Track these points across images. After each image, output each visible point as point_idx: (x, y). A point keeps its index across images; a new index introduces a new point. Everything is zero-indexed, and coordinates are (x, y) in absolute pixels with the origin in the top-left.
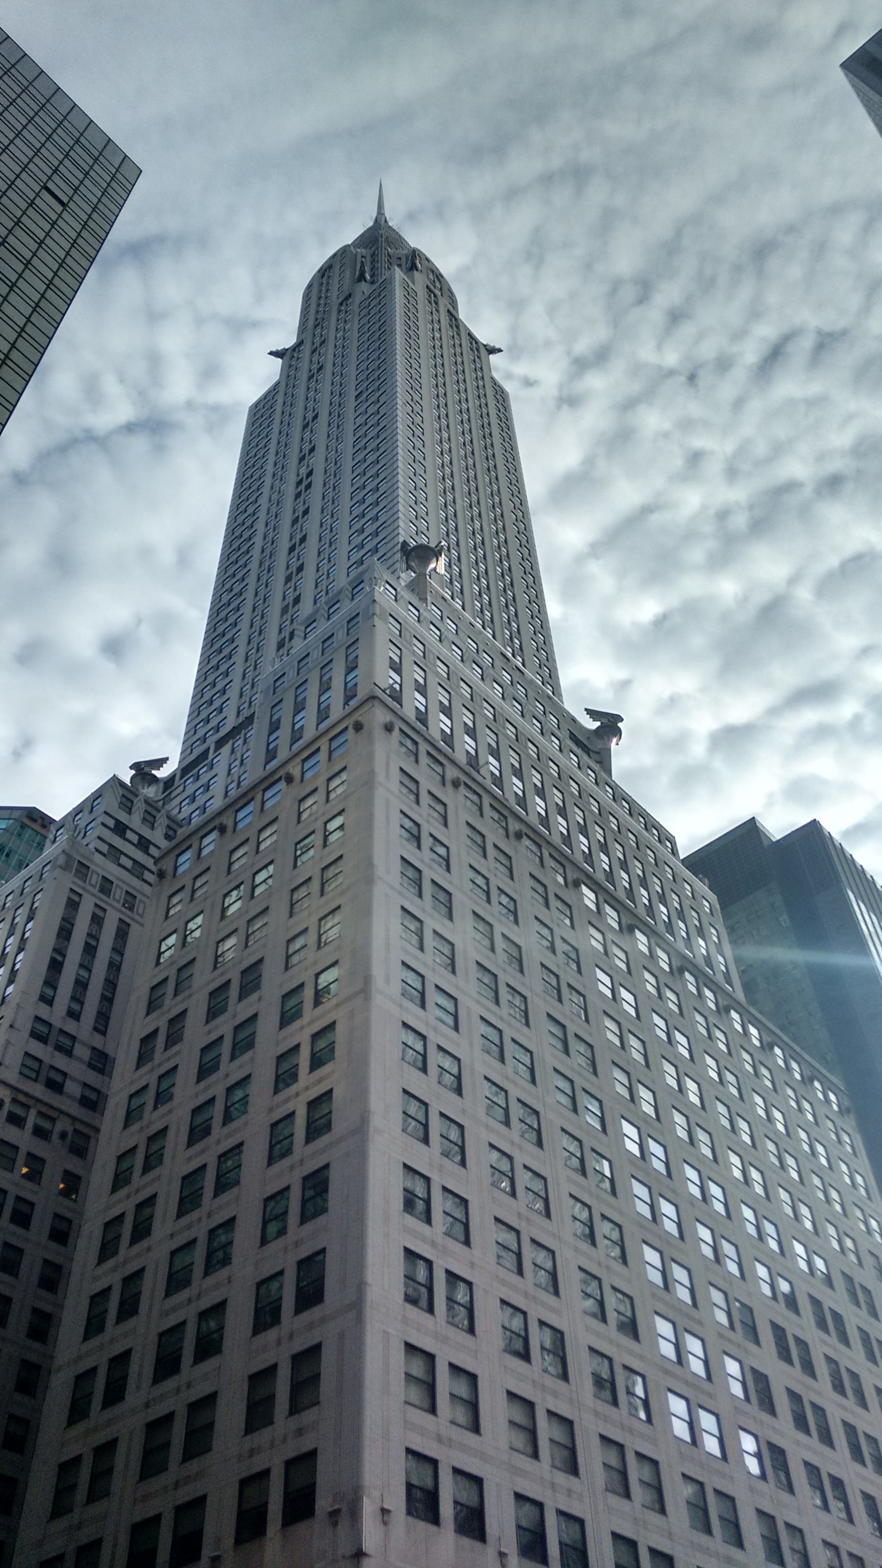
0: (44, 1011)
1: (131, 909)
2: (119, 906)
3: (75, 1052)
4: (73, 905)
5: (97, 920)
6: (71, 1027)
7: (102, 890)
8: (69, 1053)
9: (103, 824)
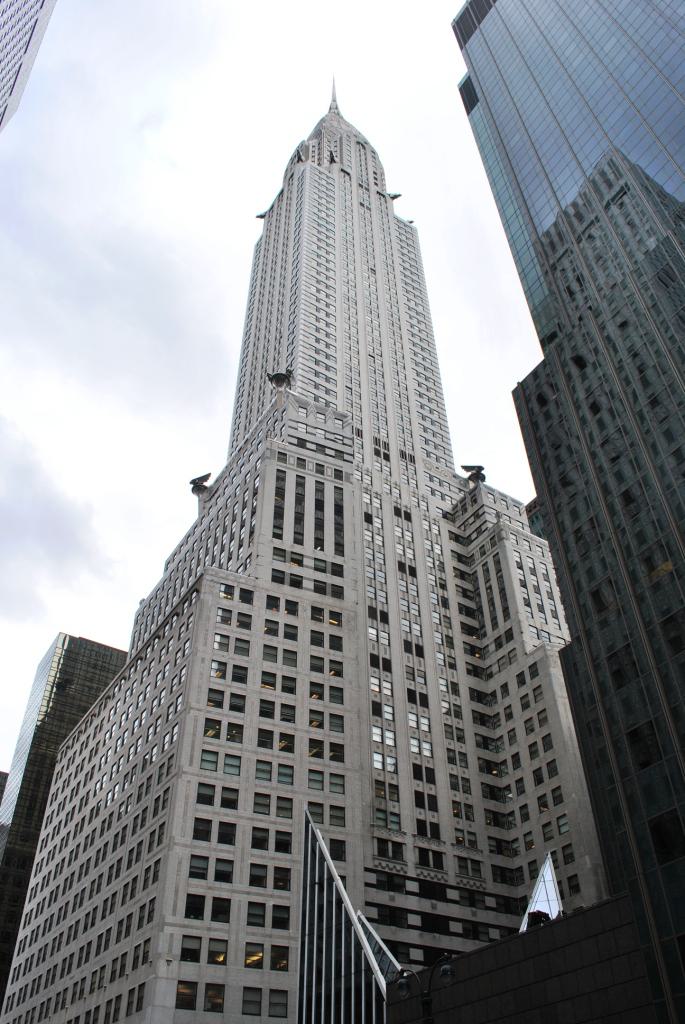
0: (277, 543)
1: (322, 473)
2: (314, 473)
3: (305, 563)
4: (281, 477)
5: (300, 483)
6: (298, 549)
7: (299, 465)
8: (300, 563)
9: (290, 427)
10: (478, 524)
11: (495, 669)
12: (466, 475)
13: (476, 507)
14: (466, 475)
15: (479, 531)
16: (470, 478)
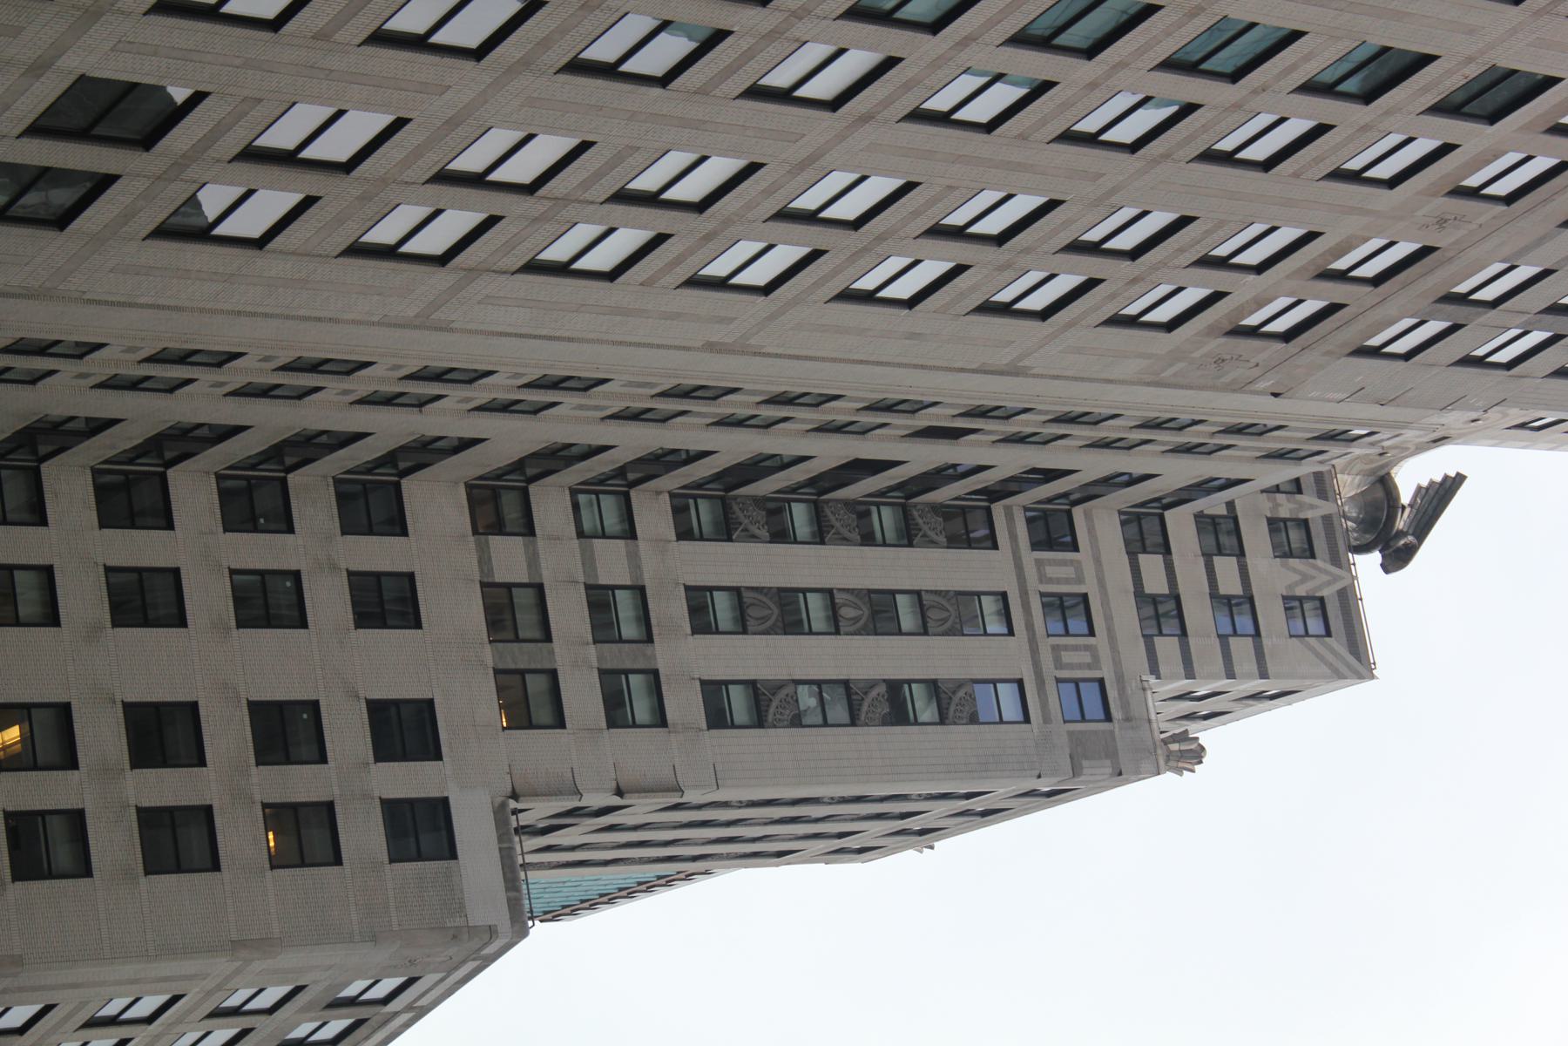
10: (1198, 611)
11: (509, 558)
12: (1410, 478)
13: (1271, 615)
14: (1410, 478)
15: (1162, 612)
16: (1385, 483)
